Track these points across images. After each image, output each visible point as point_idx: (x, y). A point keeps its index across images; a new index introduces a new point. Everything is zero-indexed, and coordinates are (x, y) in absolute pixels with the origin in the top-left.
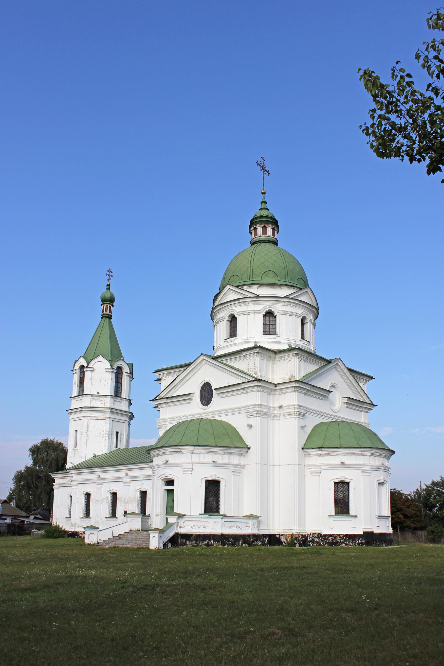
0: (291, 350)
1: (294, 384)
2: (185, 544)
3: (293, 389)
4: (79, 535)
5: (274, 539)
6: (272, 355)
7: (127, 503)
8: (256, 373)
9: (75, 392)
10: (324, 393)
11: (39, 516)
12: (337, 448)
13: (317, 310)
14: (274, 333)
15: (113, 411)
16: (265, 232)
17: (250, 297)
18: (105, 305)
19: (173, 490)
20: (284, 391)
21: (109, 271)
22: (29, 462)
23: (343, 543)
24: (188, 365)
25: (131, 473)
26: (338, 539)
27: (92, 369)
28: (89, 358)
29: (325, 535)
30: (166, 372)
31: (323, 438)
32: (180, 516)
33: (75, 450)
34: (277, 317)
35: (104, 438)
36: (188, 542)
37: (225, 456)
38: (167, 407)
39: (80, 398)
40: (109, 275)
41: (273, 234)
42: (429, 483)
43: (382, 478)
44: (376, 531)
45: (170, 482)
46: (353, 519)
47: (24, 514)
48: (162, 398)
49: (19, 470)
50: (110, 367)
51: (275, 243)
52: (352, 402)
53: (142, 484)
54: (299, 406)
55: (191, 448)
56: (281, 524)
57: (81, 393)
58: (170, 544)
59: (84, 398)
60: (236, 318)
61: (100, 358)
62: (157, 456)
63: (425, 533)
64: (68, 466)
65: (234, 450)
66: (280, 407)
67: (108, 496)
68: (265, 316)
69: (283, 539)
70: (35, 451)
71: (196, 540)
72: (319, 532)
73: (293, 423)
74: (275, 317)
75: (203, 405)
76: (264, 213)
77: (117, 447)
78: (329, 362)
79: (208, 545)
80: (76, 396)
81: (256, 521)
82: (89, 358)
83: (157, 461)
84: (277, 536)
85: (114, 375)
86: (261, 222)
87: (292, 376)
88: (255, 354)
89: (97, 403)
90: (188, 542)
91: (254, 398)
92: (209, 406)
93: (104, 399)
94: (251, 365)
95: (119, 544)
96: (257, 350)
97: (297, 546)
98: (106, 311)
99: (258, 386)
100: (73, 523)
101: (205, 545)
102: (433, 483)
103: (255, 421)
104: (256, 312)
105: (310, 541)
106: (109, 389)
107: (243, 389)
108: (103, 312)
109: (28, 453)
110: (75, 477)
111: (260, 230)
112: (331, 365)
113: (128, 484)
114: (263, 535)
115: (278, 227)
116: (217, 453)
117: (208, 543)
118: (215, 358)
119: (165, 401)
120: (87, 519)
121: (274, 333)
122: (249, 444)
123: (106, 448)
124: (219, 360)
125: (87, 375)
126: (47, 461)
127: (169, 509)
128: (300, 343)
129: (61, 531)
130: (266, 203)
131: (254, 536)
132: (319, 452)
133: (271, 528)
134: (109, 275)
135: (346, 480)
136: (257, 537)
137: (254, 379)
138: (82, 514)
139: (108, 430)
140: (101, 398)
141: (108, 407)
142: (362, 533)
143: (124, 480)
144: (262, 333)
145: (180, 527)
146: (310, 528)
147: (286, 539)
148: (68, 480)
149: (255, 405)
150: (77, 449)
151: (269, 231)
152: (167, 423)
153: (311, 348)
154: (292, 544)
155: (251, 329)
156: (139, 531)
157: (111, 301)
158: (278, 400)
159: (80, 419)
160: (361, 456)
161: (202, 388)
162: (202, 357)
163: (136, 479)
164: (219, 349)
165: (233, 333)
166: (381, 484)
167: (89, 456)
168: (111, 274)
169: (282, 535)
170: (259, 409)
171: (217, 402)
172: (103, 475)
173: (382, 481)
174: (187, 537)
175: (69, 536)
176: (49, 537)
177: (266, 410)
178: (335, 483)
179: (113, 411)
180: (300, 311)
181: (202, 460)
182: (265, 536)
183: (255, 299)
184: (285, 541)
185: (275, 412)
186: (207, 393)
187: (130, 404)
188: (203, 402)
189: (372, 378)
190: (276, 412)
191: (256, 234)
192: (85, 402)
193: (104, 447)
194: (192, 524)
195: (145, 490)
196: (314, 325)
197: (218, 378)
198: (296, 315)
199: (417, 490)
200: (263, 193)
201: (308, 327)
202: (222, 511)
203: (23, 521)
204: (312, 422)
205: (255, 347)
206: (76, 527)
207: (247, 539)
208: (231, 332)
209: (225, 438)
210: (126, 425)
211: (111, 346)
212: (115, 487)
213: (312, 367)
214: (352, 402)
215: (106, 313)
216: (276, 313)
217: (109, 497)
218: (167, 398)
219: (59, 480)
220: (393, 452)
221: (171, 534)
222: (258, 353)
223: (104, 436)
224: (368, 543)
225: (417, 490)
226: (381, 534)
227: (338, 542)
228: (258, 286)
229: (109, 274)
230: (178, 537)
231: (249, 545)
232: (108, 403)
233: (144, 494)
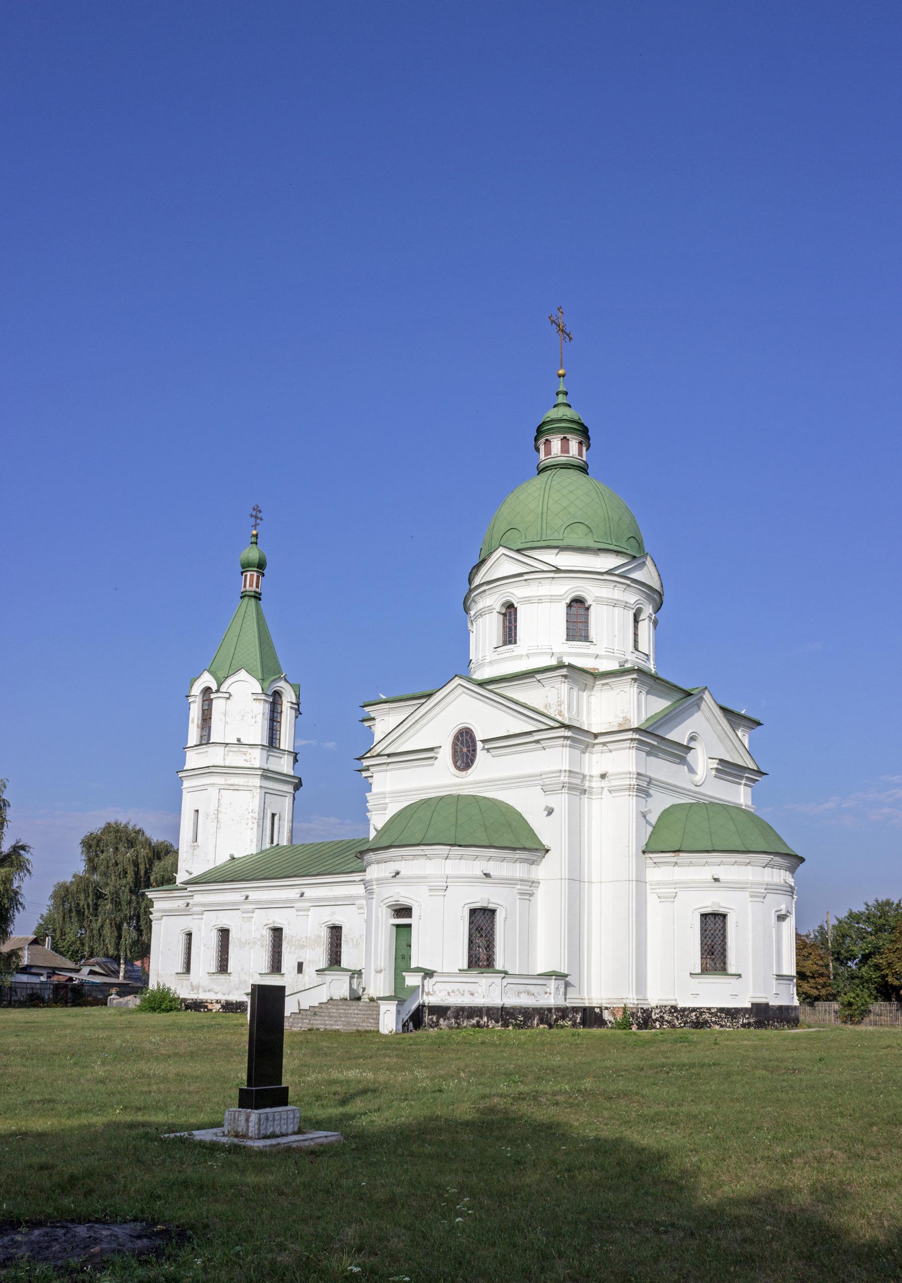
0: (622, 672)
1: (630, 735)
2: (437, 1024)
3: (627, 744)
4: (206, 1007)
5: (590, 1017)
6: (590, 680)
8: (560, 713)
9: (193, 737)
10: (680, 753)
11: (97, 969)
12: (708, 852)
13: (660, 595)
14: (586, 638)
15: (267, 775)
16: (565, 449)
17: (543, 571)
18: (249, 574)
19: (409, 926)
20: (611, 746)
21: (257, 509)
22: (80, 866)
23: (715, 1023)
24: (430, 695)
25: (310, 893)
26: (707, 1016)
27: (227, 695)
28: (221, 675)
29: (684, 1010)
31: (677, 833)
32: (429, 974)
33: (194, 848)
34: (592, 612)
35: (250, 825)
36: (441, 1021)
37: (505, 864)
38: (386, 771)
39: (203, 749)
40: (256, 517)
41: (580, 454)
42: (843, 914)
43: (783, 907)
44: (774, 1002)
45: (404, 911)
46: (733, 981)
47: (71, 965)
48: (378, 755)
49: (61, 880)
50: (260, 691)
51: (583, 469)
52: (728, 770)
53: (333, 913)
54: (638, 774)
56: (603, 987)
57: (205, 740)
58: (411, 1024)
59: (211, 749)
60: (516, 609)
61: (243, 674)
62: (378, 862)
63: (836, 1006)
64: (181, 877)
65: (519, 855)
66: (603, 776)
67: (264, 933)
68: (569, 606)
69: (607, 1016)
70: (93, 846)
71: (456, 1018)
72: (673, 1003)
73: (629, 804)
74: (588, 609)
75: (458, 768)
77: (272, 842)
78: (689, 694)
79: (478, 1025)
80: (196, 746)
81: (561, 983)
82: (221, 675)
83: (374, 872)
84: (597, 1010)
85: (268, 706)
86: (559, 430)
87: (626, 719)
88: (560, 679)
89: (235, 759)
90: (441, 1021)
91: (556, 758)
92: (470, 771)
93: (250, 751)
94: (549, 696)
95: (319, 1024)
96: (564, 671)
97: (634, 1028)
98: (251, 585)
99: (565, 737)
100: (194, 984)
101: (473, 1026)
102: (851, 915)
103: (560, 801)
104: (553, 599)
105: (656, 1020)
106: (257, 733)
107: (537, 742)
108: (245, 586)
109: (79, 849)
110: (198, 898)
111: (556, 445)
112: (691, 700)
113: (305, 910)
114: (573, 1008)
115: (589, 439)
116: (504, 859)
117: (478, 1022)
118: (482, 684)
119: (384, 760)
120: (222, 977)
121: (586, 638)
122: (546, 841)
123: (254, 845)
124: (490, 687)
125: (218, 705)
126: (117, 864)
127: (399, 960)
128: (632, 660)
129: (174, 1000)
131: (558, 1009)
132: (675, 860)
133: (585, 996)
134: (256, 517)
135: (722, 910)
136: (563, 1012)
137: (557, 725)
138: (213, 966)
139: (257, 810)
141: (258, 766)
142: (749, 1006)
144: (565, 637)
145: (428, 994)
146: (657, 996)
147: (614, 1015)
148: (181, 903)
149: (560, 771)
150: (198, 846)
151: (574, 446)
152: (387, 800)
153: (651, 667)
154: (625, 1025)
155: (543, 633)
156: (346, 999)
157: (261, 566)
158: (597, 762)
159: (203, 789)
160: (749, 867)
161: (456, 738)
162: (457, 681)
163: (319, 903)
164: (481, 665)
165: (510, 636)
166: (781, 918)
167: (222, 859)
168: (259, 515)
169: (606, 1008)
170: (566, 780)
171: (486, 765)
172: (254, 895)
173: (783, 912)
174: (440, 1011)
175: (188, 1007)
176: (153, 1009)
177: (578, 781)
178: (702, 915)
179: (267, 775)
180: (632, 598)
181: (463, 872)
182: (575, 1009)
183: (552, 575)
184: (611, 1019)
185: (594, 784)
186: (465, 748)
187: (296, 760)
188: (459, 763)
189: (759, 724)
190: (596, 783)
191: (548, 452)
192: (213, 756)
193: (249, 842)
194: (450, 987)
195: (338, 923)
196: (655, 623)
197: (488, 720)
198: (626, 606)
199: (821, 927)
201: (645, 627)
202: (499, 965)
203: (71, 979)
204: (660, 802)
205: (561, 666)
206: (201, 990)
207: (544, 1015)
208: (504, 636)
209: (501, 832)
210: (288, 801)
211: (261, 651)
212: (277, 918)
213: (659, 704)
214: (728, 770)
215: (251, 589)
216: (589, 602)
217: (267, 935)
218: (389, 755)
219: (161, 903)
220: (802, 860)
221: (414, 1007)
222: (565, 676)
223: (250, 821)
224: (760, 1024)
225: (821, 927)
226: (781, 1007)
227: (706, 1022)
228: (556, 551)
229: (256, 515)
230: (423, 1012)
231: (551, 1027)
232: (256, 758)
233: (336, 931)
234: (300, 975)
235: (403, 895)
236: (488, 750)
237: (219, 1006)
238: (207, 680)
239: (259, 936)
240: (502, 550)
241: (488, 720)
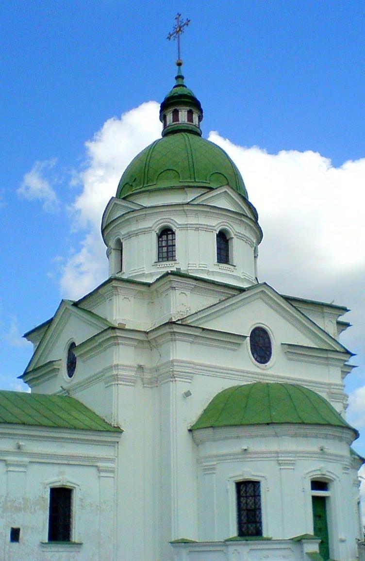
7: (18, 509)
45: (319, 484)
53: (62, 473)
76: (179, 91)
86: (185, 104)
111: (195, 117)
130: (182, 77)
137: (342, 350)
143: (9, 458)
218: (204, 329)
234: (15, 544)
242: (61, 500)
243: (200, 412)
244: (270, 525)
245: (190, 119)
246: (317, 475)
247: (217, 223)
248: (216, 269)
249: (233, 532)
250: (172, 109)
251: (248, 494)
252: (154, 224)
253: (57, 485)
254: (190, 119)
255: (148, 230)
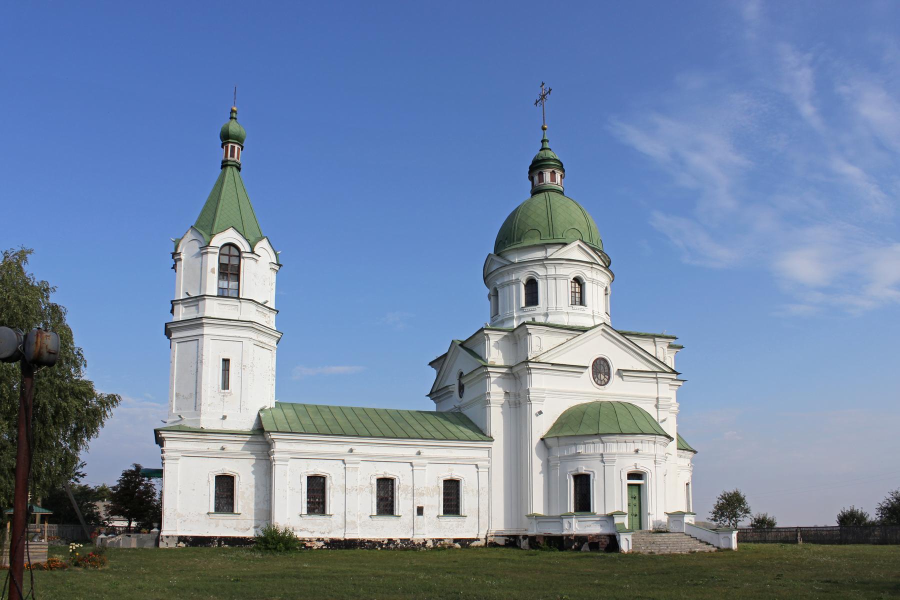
7: (422, 494)
18: (230, 145)
24: (584, 330)
30: (548, 329)
53: (452, 470)
55: (618, 438)
108: (232, 155)
120: (318, 519)
125: (247, 265)
140: (266, 311)
150: (231, 394)
159: (239, 340)
200: (544, 129)
218: (553, 364)
234: (420, 517)
235: (642, 465)
236: (621, 377)
237: (322, 543)
238: (231, 236)
239: (367, 484)
240: (578, 242)
241: (619, 357)
242: (452, 489)
243: (551, 425)
244: (597, 506)
245: (553, 179)
246: (632, 469)
247: (572, 272)
248: (570, 310)
249: (571, 508)
250: (538, 172)
251: (583, 482)
252: (523, 277)
253: (448, 478)
254: (553, 179)
255: (517, 281)
